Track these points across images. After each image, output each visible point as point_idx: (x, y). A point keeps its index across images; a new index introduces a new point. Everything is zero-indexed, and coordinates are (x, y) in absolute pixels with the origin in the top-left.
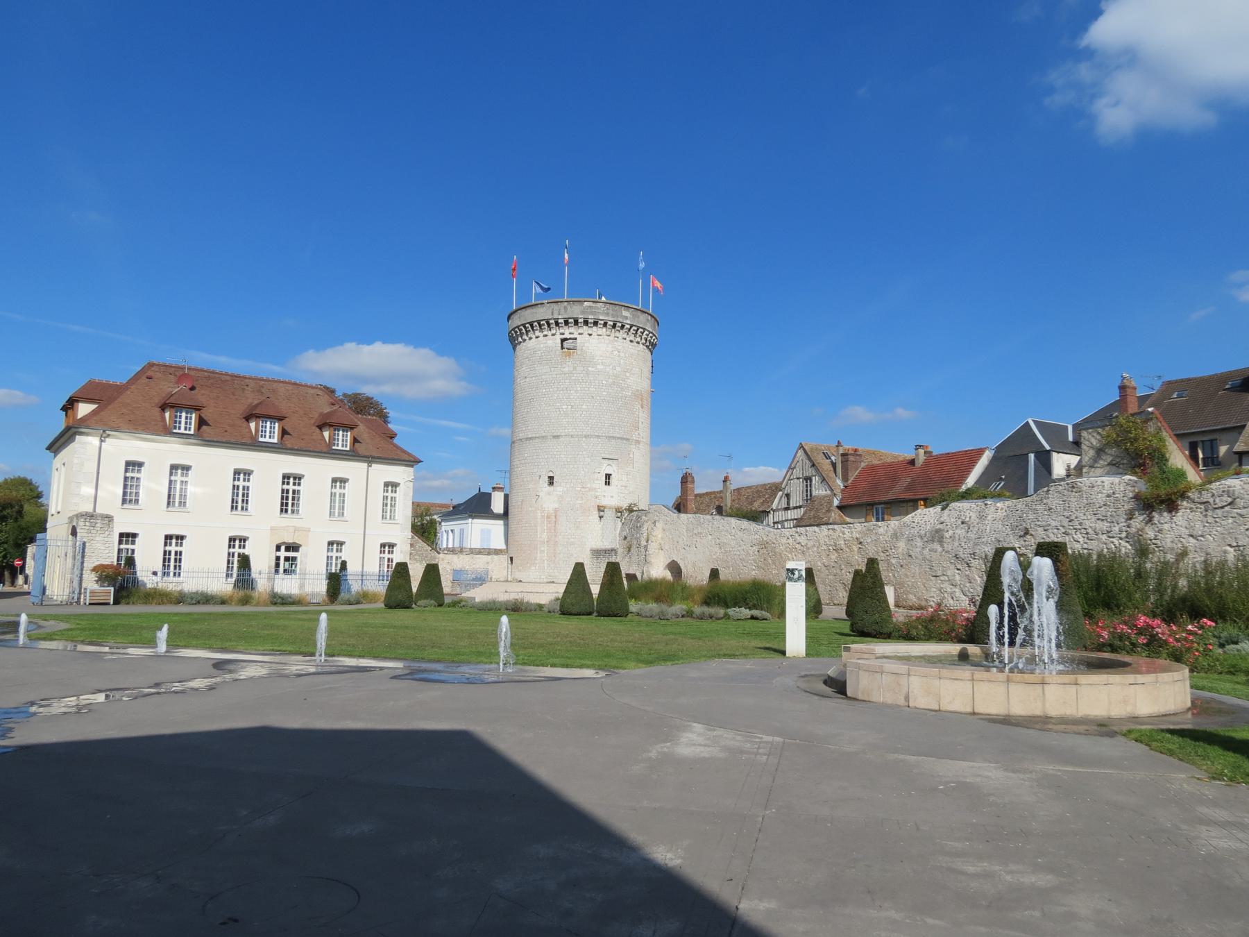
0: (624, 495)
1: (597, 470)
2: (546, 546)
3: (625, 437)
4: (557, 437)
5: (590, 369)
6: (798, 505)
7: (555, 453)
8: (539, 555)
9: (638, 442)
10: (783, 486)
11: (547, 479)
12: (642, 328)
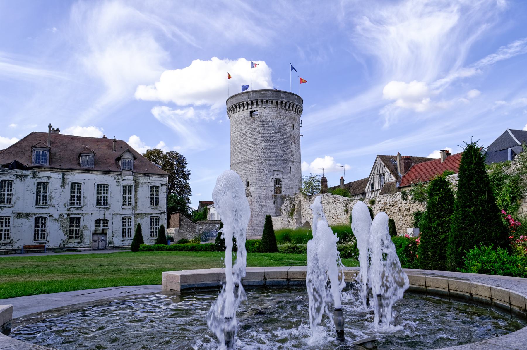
0: (286, 189)
1: (271, 177)
3: (285, 159)
4: (251, 161)
5: (265, 125)
6: (378, 189)
7: (250, 169)
9: (293, 162)
10: (370, 179)
11: (245, 183)
12: (292, 103)
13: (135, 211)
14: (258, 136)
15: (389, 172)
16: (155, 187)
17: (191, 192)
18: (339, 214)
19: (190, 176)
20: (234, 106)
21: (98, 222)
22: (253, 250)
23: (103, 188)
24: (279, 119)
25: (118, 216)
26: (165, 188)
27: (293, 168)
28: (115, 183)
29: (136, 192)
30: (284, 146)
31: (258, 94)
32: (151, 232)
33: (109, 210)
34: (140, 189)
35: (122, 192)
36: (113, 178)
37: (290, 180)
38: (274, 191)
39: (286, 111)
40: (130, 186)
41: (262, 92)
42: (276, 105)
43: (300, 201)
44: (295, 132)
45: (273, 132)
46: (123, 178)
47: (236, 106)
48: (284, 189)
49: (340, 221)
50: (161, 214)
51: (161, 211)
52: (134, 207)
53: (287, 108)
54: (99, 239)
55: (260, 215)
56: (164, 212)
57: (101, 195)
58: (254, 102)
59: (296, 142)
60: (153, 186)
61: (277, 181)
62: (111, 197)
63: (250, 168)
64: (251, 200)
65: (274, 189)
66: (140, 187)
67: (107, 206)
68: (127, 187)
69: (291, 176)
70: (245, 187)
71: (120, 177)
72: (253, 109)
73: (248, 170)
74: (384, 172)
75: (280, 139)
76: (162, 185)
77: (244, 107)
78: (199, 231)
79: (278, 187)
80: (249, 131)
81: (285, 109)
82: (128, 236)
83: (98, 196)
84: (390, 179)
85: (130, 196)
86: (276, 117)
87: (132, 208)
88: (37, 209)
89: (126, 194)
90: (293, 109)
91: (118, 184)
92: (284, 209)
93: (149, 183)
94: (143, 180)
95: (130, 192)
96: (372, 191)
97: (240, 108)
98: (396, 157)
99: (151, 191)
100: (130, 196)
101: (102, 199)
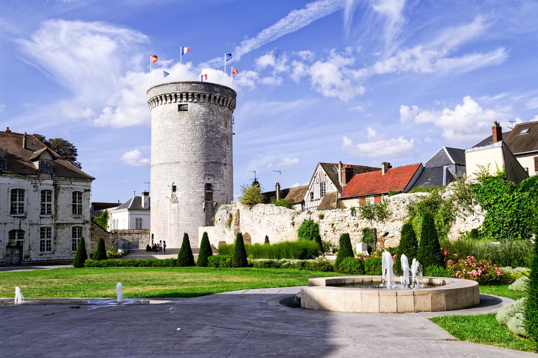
2: (173, 227)
4: (178, 163)
6: (318, 198)
7: (177, 172)
8: (169, 232)
9: (225, 164)
10: (310, 188)
11: (171, 187)
13: (55, 221)
14: (187, 134)
15: (331, 182)
16: (77, 194)
18: (285, 227)
20: (158, 97)
21: (12, 234)
22: (225, 265)
23: (18, 194)
24: (212, 116)
25: (36, 226)
27: (225, 171)
28: (32, 188)
29: (56, 198)
30: (216, 146)
32: (73, 245)
33: (26, 219)
34: (60, 195)
35: (40, 198)
36: (30, 182)
37: (222, 185)
38: (204, 197)
39: (219, 107)
40: (50, 192)
42: (208, 100)
43: (238, 211)
44: (228, 131)
46: (42, 183)
47: (161, 97)
48: (215, 195)
49: (286, 234)
50: (84, 224)
51: (84, 220)
52: (54, 216)
53: (221, 103)
54: (12, 253)
55: (189, 225)
56: (87, 222)
57: (15, 202)
58: (184, 95)
60: (76, 192)
61: (208, 186)
62: (27, 204)
63: (178, 170)
64: (178, 207)
65: (204, 195)
66: (60, 192)
67: (23, 215)
68: (46, 192)
69: (223, 180)
71: (38, 181)
72: (183, 103)
73: (175, 172)
74: (324, 181)
75: (213, 139)
77: (171, 99)
78: (113, 242)
79: (209, 192)
80: (177, 128)
81: (218, 104)
82: (47, 250)
83: (12, 204)
84: (331, 189)
85: (49, 203)
86: (208, 113)
87: (52, 217)
89: (45, 201)
90: (226, 105)
91: (36, 189)
92: (218, 218)
93: (71, 188)
94: (64, 184)
95: (49, 199)
96: (312, 201)
97: (166, 100)
98: (337, 165)
99: (73, 198)
100: (49, 203)
101: (18, 206)
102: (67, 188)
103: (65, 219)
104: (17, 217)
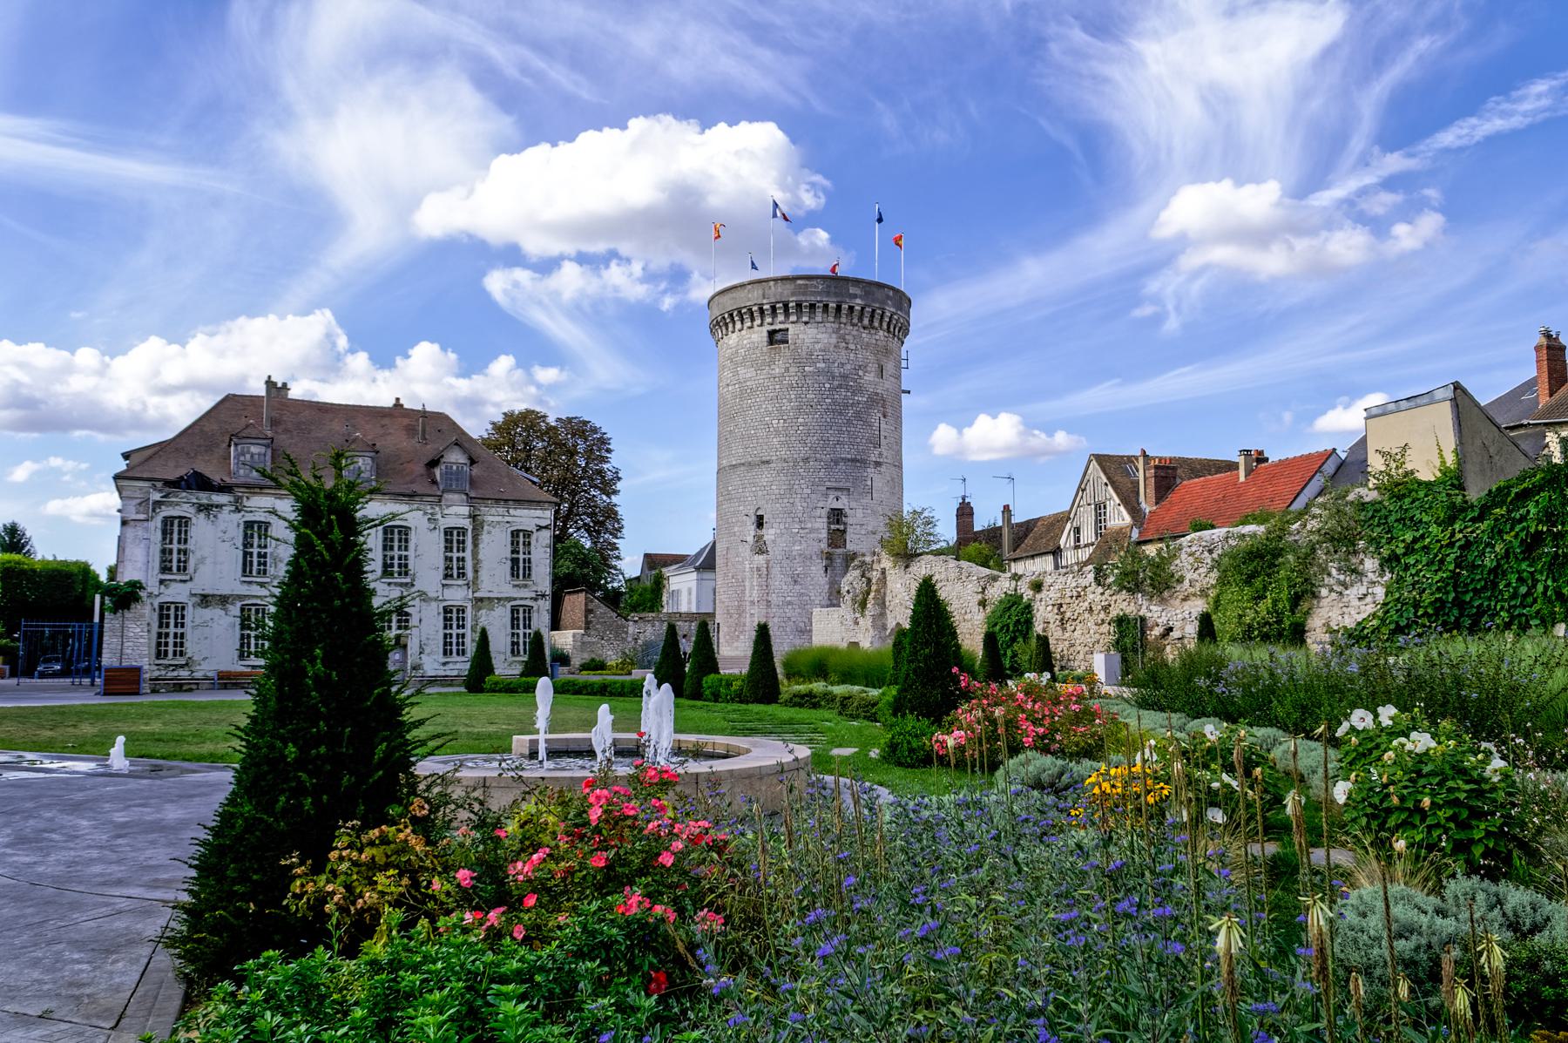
1: (820, 504)
4: (768, 462)
8: (748, 620)
9: (878, 464)
11: (754, 518)
15: (1118, 501)
17: (622, 527)
19: (619, 486)
23: (396, 537)
24: (843, 352)
25: (434, 604)
26: (545, 537)
27: (878, 479)
29: (476, 545)
31: (789, 287)
32: (513, 644)
35: (442, 545)
38: (825, 541)
40: (462, 531)
41: (799, 282)
42: (835, 317)
43: (883, 572)
45: (827, 386)
47: (731, 315)
50: (536, 599)
53: (866, 322)
56: (543, 596)
59: (889, 411)
60: (518, 531)
61: (836, 515)
64: (768, 562)
66: (485, 532)
67: (408, 580)
68: (455, 533)
70: (750, 531)
72: (778, 327)
75: (846, 406)
76: (540, 528)
77: (753, 320)
82: (458, 654)
83: (385, 556)
84: (1119, 518)
88: (246, 587)
89: (451, 551)
94: (492, 514)
96: (1077, 547)
97: (742, 321)
98: (1136, 458)
101: (396, 562)
102: (498, 522)
103: (495, 589)
104: (396, 584)
